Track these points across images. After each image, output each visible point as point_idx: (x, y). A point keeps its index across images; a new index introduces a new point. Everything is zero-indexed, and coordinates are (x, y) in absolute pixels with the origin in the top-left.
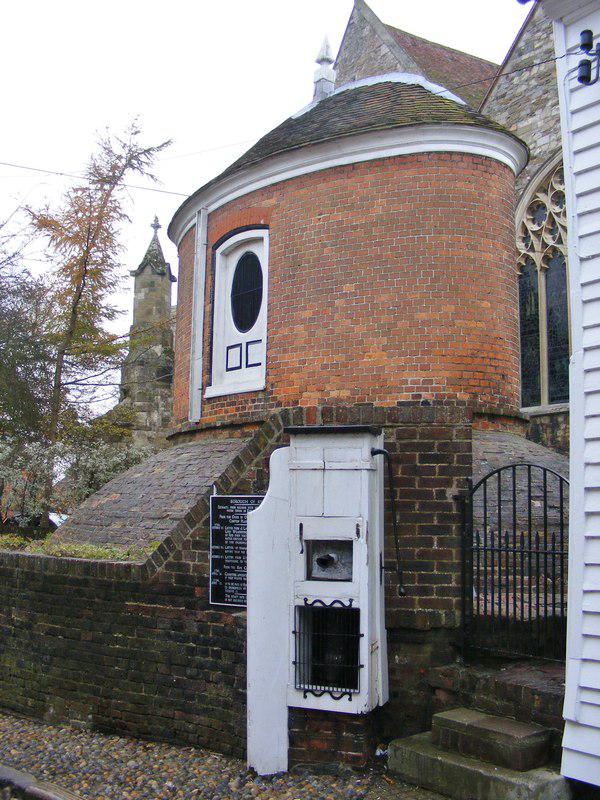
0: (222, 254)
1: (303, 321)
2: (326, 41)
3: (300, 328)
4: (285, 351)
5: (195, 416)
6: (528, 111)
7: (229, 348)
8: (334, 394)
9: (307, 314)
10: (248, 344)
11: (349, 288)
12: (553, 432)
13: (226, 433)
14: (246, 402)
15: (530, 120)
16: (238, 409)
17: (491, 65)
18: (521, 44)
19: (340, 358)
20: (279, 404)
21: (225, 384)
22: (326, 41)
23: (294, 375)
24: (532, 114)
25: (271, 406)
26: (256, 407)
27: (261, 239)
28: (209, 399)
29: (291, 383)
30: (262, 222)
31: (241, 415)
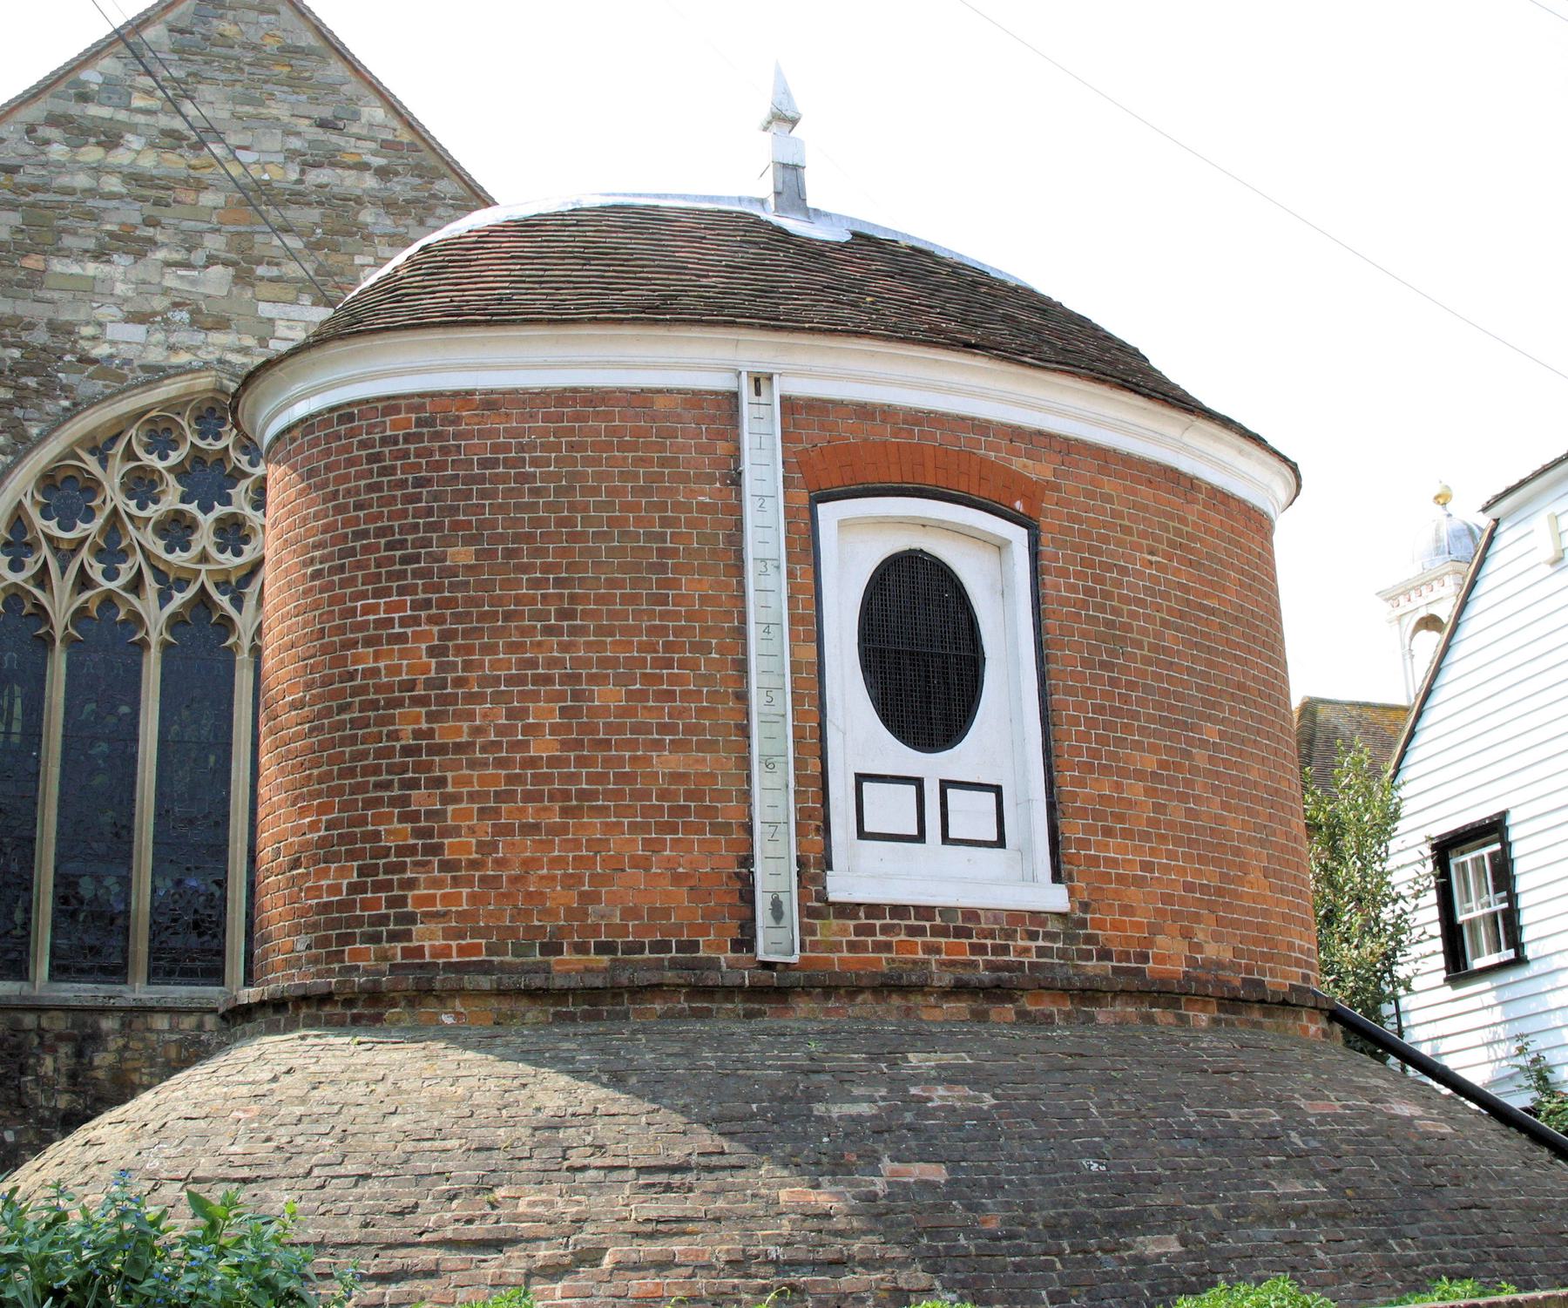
0: (844, 524)
1: (1140, 775)
2: (777, 64)
3: (1135, 790)
4: (1108, 832)
5: (776, 941)
6: (91, 244)
7: (861, 778)
8: (1212, 951)
9: (1150, 762)
10: (945, 785)
11: (1210, 732)
12: (79, 1054)
13: (959, 1007)
14: (1010, 935)
15: (92, 268)
16: (979, 949)
17: (424, 171)
18: (92, 76)
19: (1209, 876)
20: (1105, 955)
21: (862, 875)
22: (777, 64)
23: (1134, 895)
24: (100, 255)
25: (1087, 956)
26: (1041, 952)
27: (1000, 546)
28: (846, 910)
29: (1127, 910)
30: (1018, 505)
31: (990, 966)
